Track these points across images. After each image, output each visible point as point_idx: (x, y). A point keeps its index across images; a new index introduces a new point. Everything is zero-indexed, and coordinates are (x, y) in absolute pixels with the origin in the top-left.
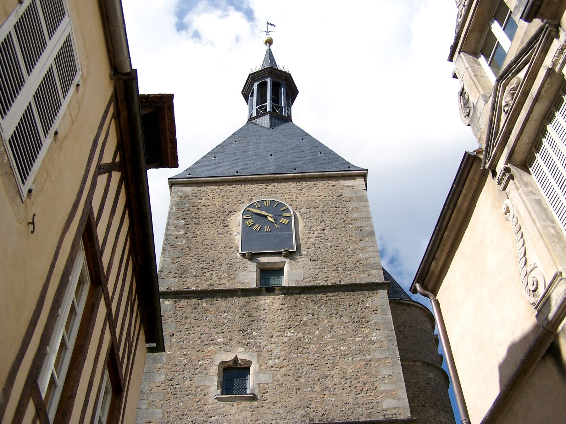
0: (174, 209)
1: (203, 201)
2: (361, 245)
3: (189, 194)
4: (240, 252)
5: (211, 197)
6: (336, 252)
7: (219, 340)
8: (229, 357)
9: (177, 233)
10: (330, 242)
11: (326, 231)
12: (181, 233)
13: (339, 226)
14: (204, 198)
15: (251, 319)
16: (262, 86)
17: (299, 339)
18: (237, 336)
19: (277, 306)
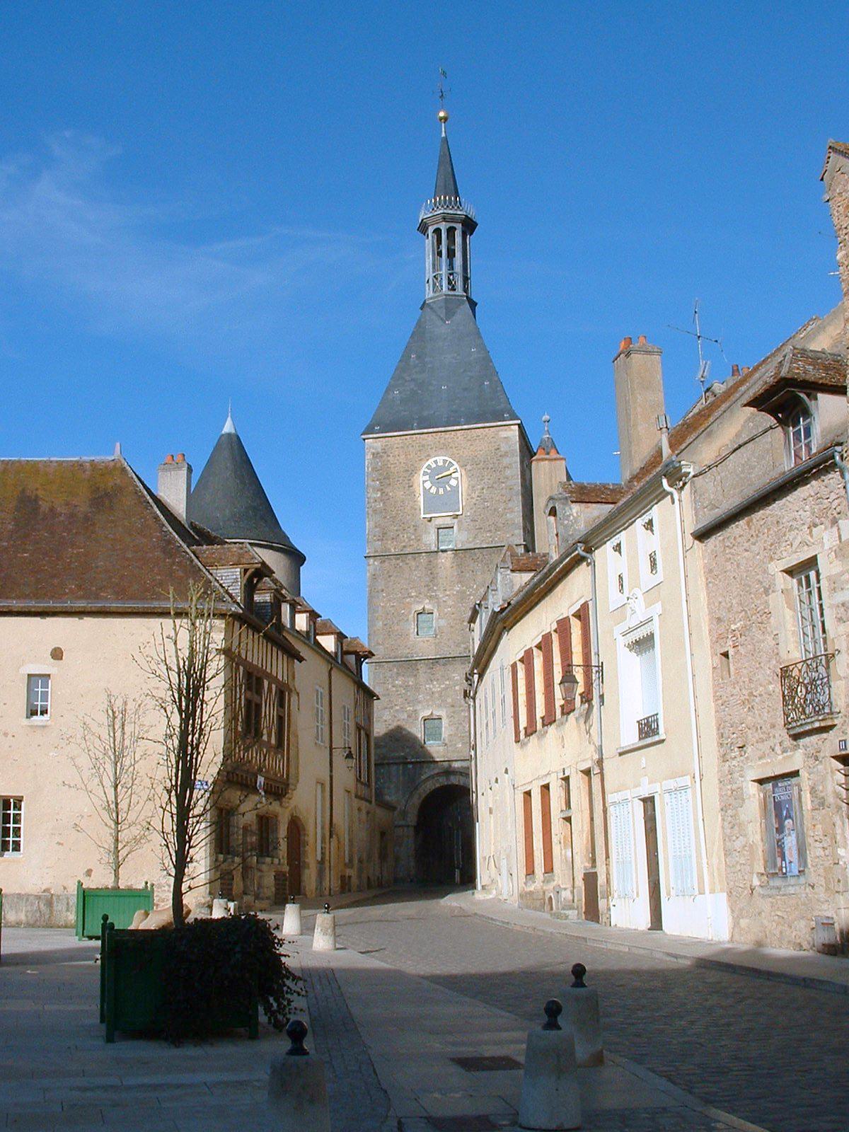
0: (370, 469)
1: (391, 458)
2: (510, 506)
3: (380, 450)
4: (422, 516)
5: (397, 453)
6: (490, 512)
7: (413, 594)
8: (420, 608)
9: (375, 496)
10: (487, 502)
11: (484, 491)
12: (378, 495)
13: (495, 486)
14: (391, 455)
15: (433, 577)
16: (438, 231)
17: (464, 592)
18: (424, 590)
19: (448, 565)
